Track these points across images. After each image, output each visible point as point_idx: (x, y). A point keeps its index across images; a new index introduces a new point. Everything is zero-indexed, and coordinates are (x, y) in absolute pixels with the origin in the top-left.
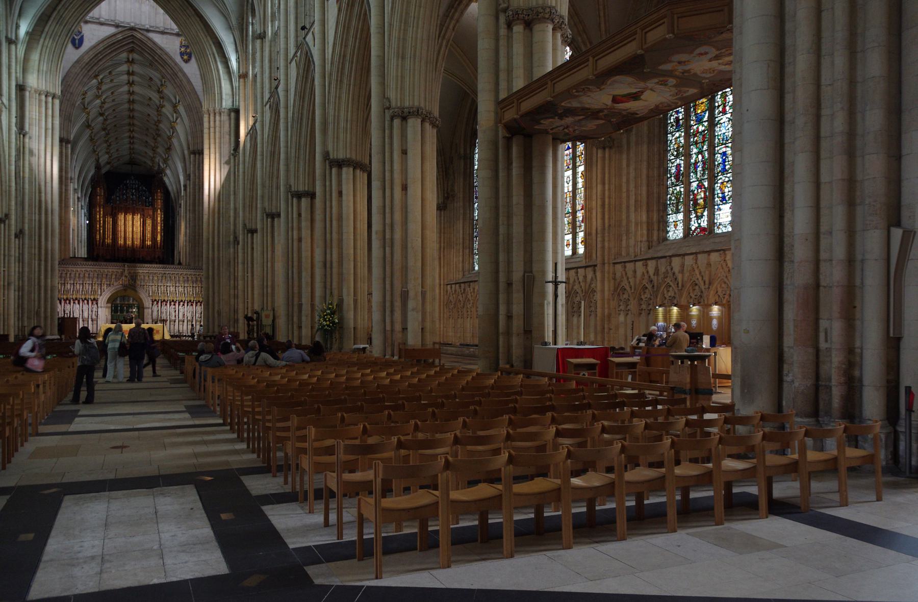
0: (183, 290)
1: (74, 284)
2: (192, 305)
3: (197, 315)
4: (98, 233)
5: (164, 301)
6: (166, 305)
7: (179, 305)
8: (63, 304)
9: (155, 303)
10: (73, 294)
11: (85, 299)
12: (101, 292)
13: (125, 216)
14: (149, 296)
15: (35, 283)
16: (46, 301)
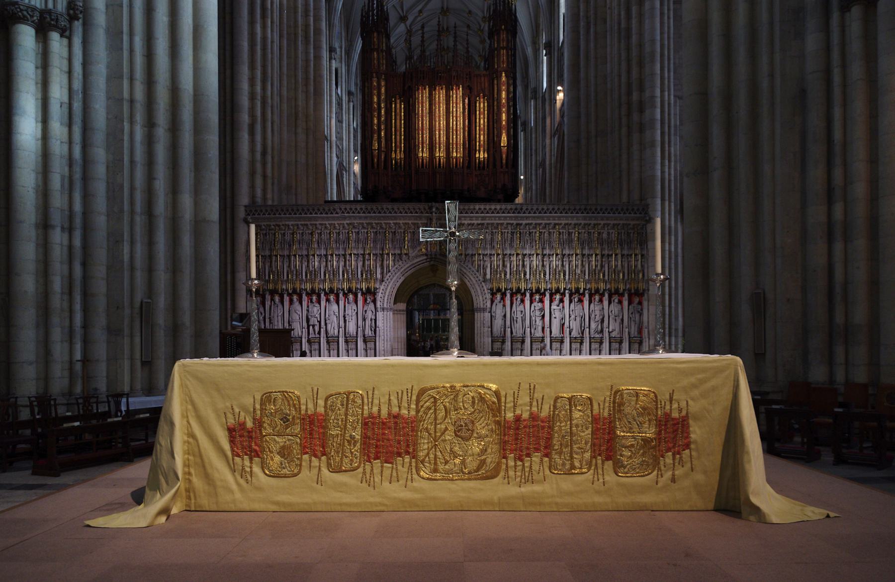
0: (560, 263)
1: (326, 256)
2: (581, 301)
3: (593, 326)
4: (376, 136)
5: (518, 291)
6: (523, 301)
7: (551, 301)
8: (305, 303)
9: (499, 296)
10: (325, 280)
11: (350, 290)
12: (382, 273)
13: (431, 94)
14: (485, 281)
15: (132, 203)
16: (175, 268)
